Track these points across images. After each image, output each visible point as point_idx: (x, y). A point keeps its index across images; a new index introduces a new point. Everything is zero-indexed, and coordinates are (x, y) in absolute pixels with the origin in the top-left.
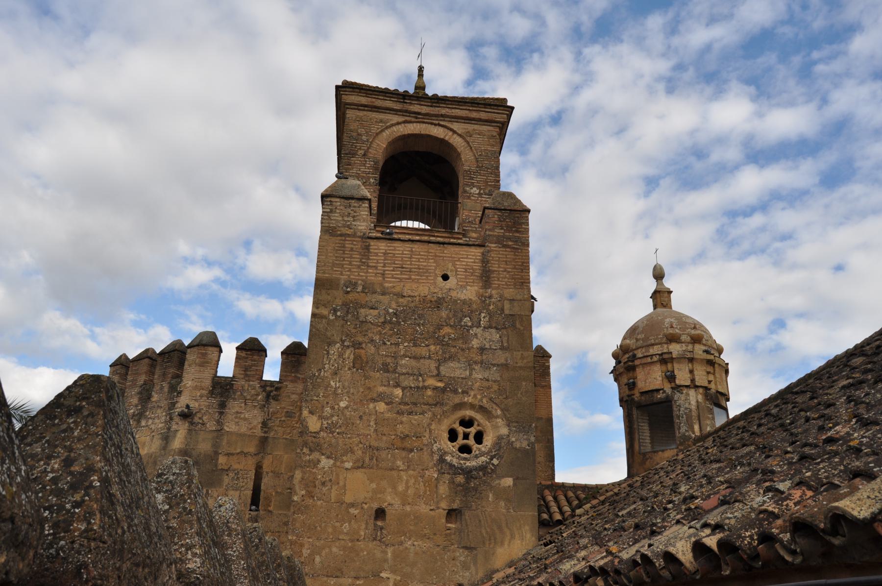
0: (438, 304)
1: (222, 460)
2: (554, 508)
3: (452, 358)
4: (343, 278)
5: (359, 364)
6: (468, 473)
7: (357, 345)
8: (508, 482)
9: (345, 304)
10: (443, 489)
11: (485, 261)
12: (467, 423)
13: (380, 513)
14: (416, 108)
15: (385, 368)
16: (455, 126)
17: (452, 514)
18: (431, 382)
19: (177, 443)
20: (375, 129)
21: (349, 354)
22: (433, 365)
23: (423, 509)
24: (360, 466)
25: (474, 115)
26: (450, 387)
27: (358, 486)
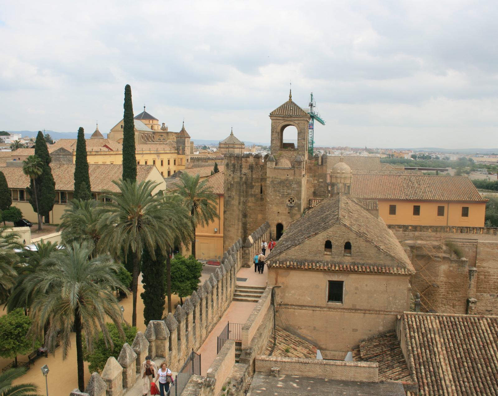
0: (287, 180)
1: (253, 183)
2: (313, 205)
3: (289, 189)
4: (271, 177)
5: (275, 191)
6: (291, 207)
7: (274, 188)
8: (297, 208)
9: (272, 181)
10: (287, 209)
11: (294, 172)
12: (291, 199)
13: (279, 213)
14: (286, 119)
15: (278, 191)
16: (296, 122)
17: (289, 213)
18: (286, 193)
19: (244, 179)
20: (278, 124)
21: (273, 189)
22: (285, 191)
23: (284, 212)
24: (275, 206)
25: (300, 119)
26: (289, 194)
27: (275, 209)
